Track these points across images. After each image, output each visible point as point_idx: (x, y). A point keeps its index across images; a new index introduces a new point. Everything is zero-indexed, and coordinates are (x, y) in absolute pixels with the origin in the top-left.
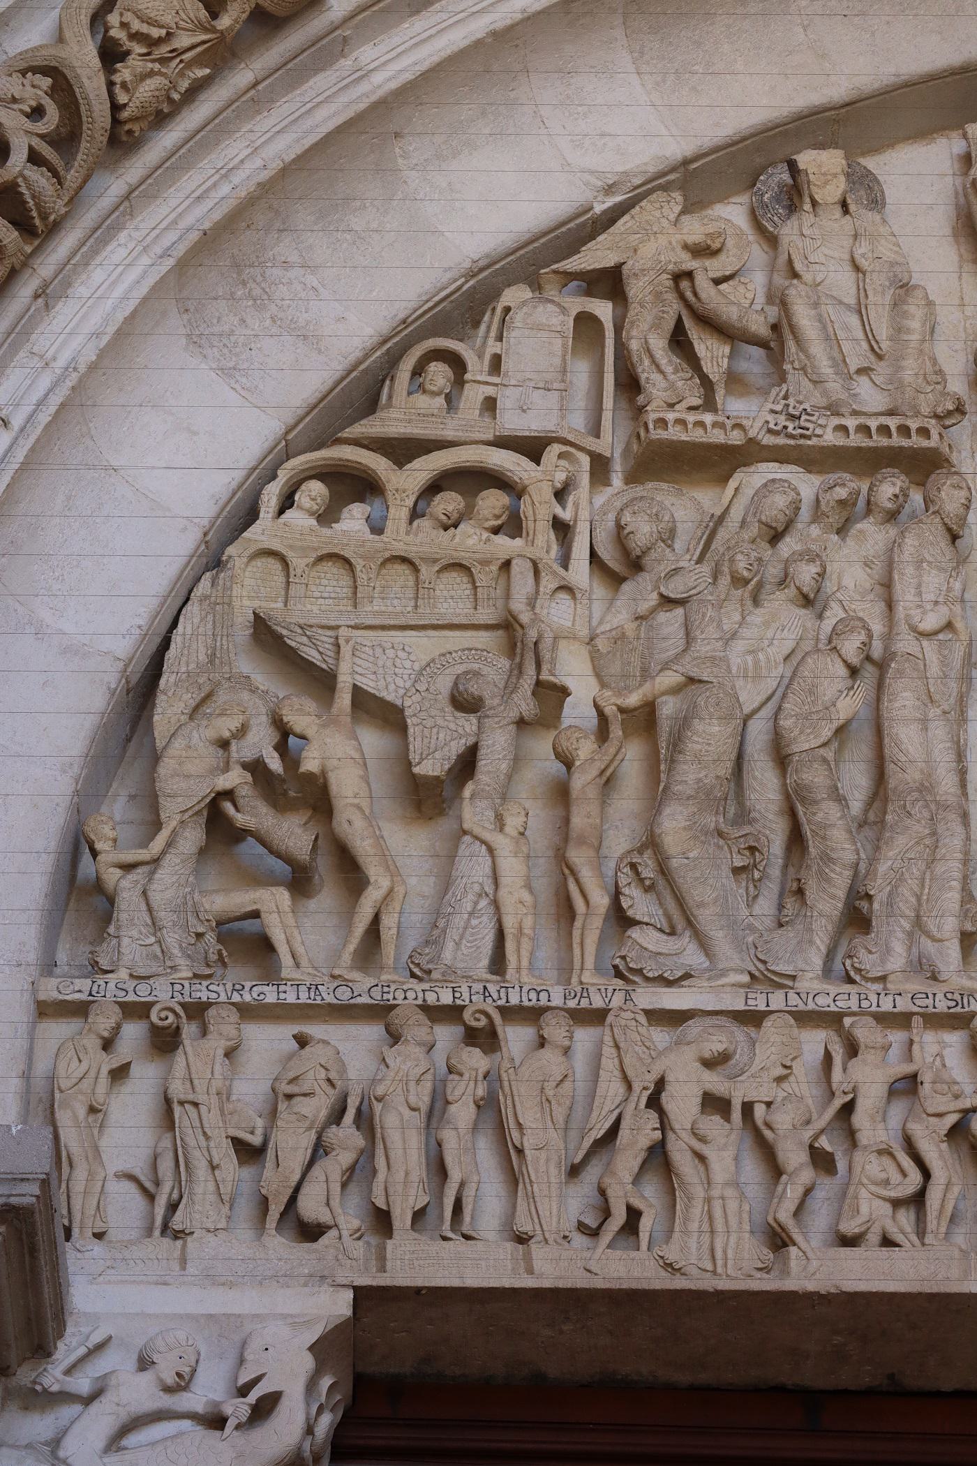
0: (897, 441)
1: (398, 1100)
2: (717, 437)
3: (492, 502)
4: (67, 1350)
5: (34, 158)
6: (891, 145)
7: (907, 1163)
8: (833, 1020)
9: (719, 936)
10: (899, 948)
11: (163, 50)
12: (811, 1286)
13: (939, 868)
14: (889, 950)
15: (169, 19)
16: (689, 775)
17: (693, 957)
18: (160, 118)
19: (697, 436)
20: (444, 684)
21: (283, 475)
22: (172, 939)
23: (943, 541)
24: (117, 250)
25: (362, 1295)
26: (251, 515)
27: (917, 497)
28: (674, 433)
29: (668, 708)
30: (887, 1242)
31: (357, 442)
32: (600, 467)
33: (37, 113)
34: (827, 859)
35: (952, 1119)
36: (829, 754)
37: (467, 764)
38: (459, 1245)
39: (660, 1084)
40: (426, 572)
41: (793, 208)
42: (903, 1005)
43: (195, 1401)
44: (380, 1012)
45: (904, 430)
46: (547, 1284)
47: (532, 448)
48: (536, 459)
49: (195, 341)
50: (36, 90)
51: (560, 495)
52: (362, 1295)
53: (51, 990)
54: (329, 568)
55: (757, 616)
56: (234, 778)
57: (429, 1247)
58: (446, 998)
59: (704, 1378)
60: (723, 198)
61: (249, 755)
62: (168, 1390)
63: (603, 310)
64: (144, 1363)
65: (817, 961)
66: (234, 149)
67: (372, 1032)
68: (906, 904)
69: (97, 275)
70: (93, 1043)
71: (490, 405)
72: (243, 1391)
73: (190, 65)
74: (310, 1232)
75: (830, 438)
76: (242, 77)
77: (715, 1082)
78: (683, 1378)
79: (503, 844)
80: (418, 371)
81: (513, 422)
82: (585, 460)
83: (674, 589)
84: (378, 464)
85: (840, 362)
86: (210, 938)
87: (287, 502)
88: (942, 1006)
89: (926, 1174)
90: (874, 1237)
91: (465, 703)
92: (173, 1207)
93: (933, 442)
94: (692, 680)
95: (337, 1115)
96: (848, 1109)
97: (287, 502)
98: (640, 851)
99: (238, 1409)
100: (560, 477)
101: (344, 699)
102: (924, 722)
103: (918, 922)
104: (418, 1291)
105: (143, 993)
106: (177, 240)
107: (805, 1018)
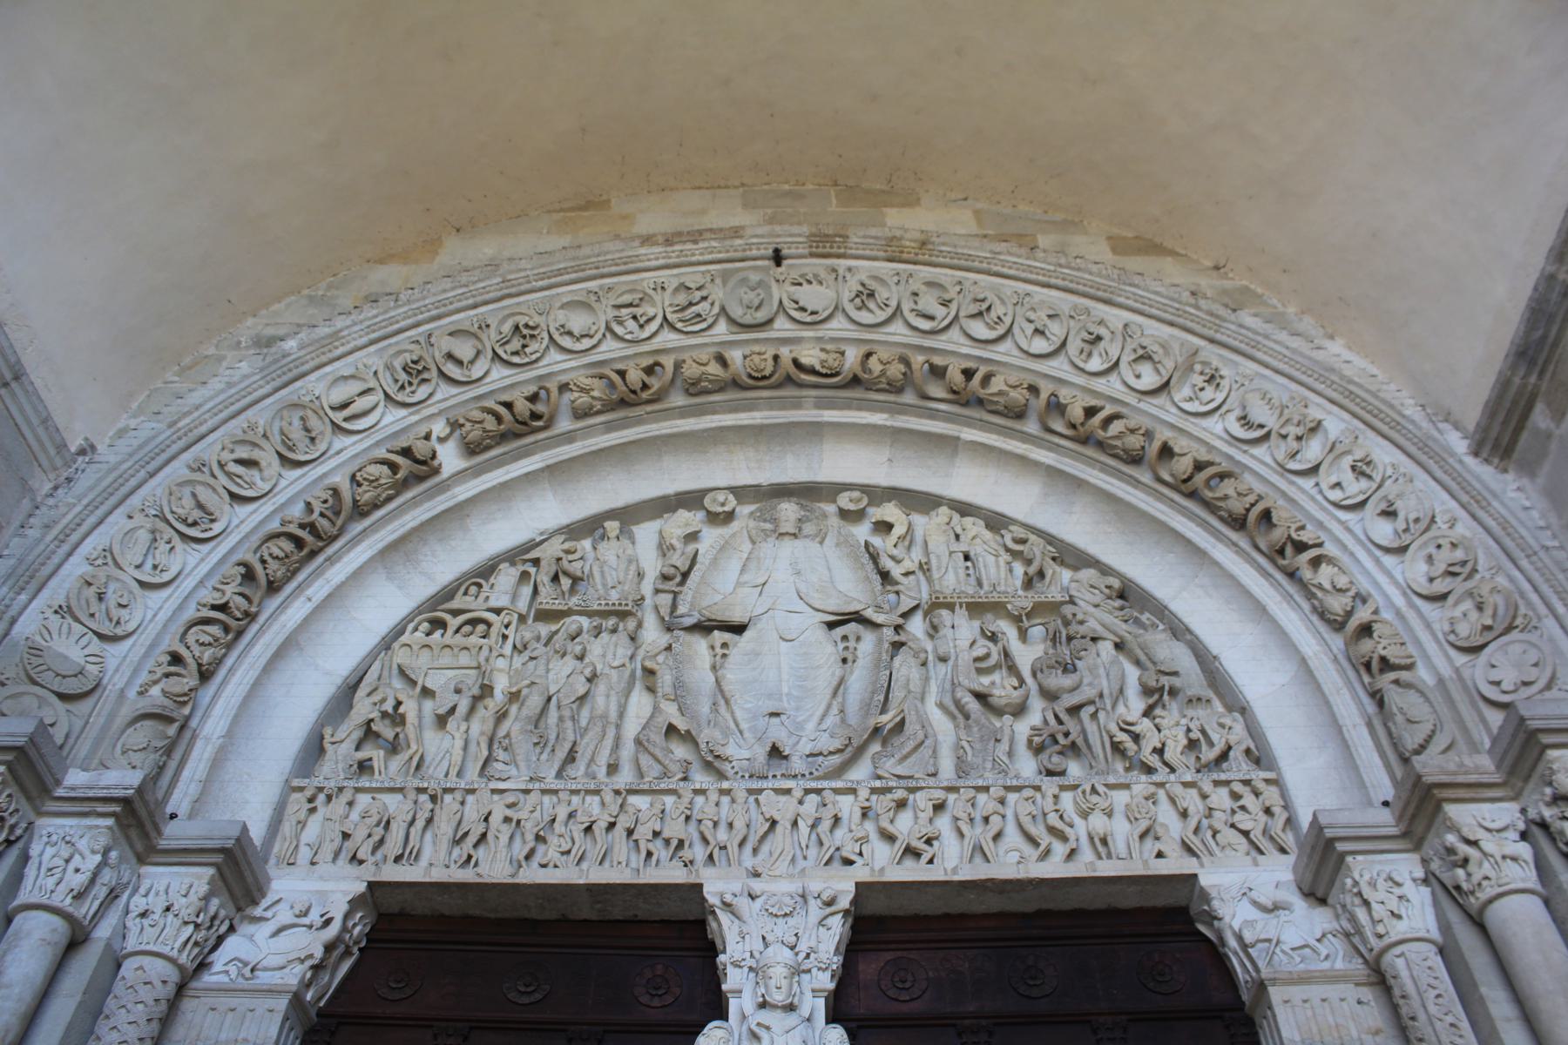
0: (617, 608)
1: (399, 819)
2: (560, 607)
3: (481, 628)
4: (265, 903)
5: (322, 515)
6: (642, 522)
7: (568, 840)
8: (555, 792)
9: (522, 765)
10: (582, 769)
11: (375, 484)
12: (524, 881)
13: (604, 742)
14: (578, 769)
15: (377, 474)
16: (525, 712)
17: (514, 772)
18: (376, 506)
19: (554, 607)
20: (452, 687)
21: (416, 621)
22: (340, 766)
23: (627, 640)
24: (359, 548)
25: (372, 886)
26: (402, 632)
27: (621, 625)
28: (547, 607)
29: (525, 692)
30: (556, 866)
31: (443, 611)
32: (522, 618)
33: (325, 502)
34: (564, 739)
35: (587, 824)
36: (574, 706)
37: (453, 710)
38: (408, 867)
39: (490, 813)
40: (456, 650)
41: (603, 539)
42: (579, 787)
43: (306, 921)
44: (401, 790)
45: (620, 604)
46: (433, 880)
47: (498, 611)
48: (498, 614)
49: (389, 578)
50: (327, 495)
51: (507, 627)
52: (372, 886)
53: (296, 783)
54: (426, 649)
55: (561, 662)
56: (375, 715)
57: (398, 867)
58: (426, 785)
59: (499, 915)
60: (584, 538)
61: (383, 709)
62: (297, 916)
63: (532, 570)
64: (292, 907)
65: (553, 773)
66: (407, 517)
67: (399, 797)
68: (588, 755)
69: (352, 555)
70: (304, 800)
71: (488, 598)
72: (322, 916)
73: (386, 489)
74: (361, 862)
75: (595, 607)
76: (409, 495)
77: (509, 813)
78: (492, 916)
79: (457, 735)
80: (467, 589)
81: (493, 603)
82: (516, 616)
83: (533, 655)
84: (447, 617)
85: (604, 585)
86: (355, 766)
87: (416, 629)
88: (592, 787)
89: (574, 843)
90: (551, 864)
91: (458, 691)
92: (316, 853)
93: (629, 608)
94: (533, 683)
95: (378, 825)
96: (554, 820)
97: (416, 629)
98: (505, 737)
99: (318, 922)
100: (506, 621)
101: (418, 689)
102: (608, 696)
103: (592, 760)
104: (389, 884)
105: (326, 784)
106: (380, 546)
107: (544, 792)
